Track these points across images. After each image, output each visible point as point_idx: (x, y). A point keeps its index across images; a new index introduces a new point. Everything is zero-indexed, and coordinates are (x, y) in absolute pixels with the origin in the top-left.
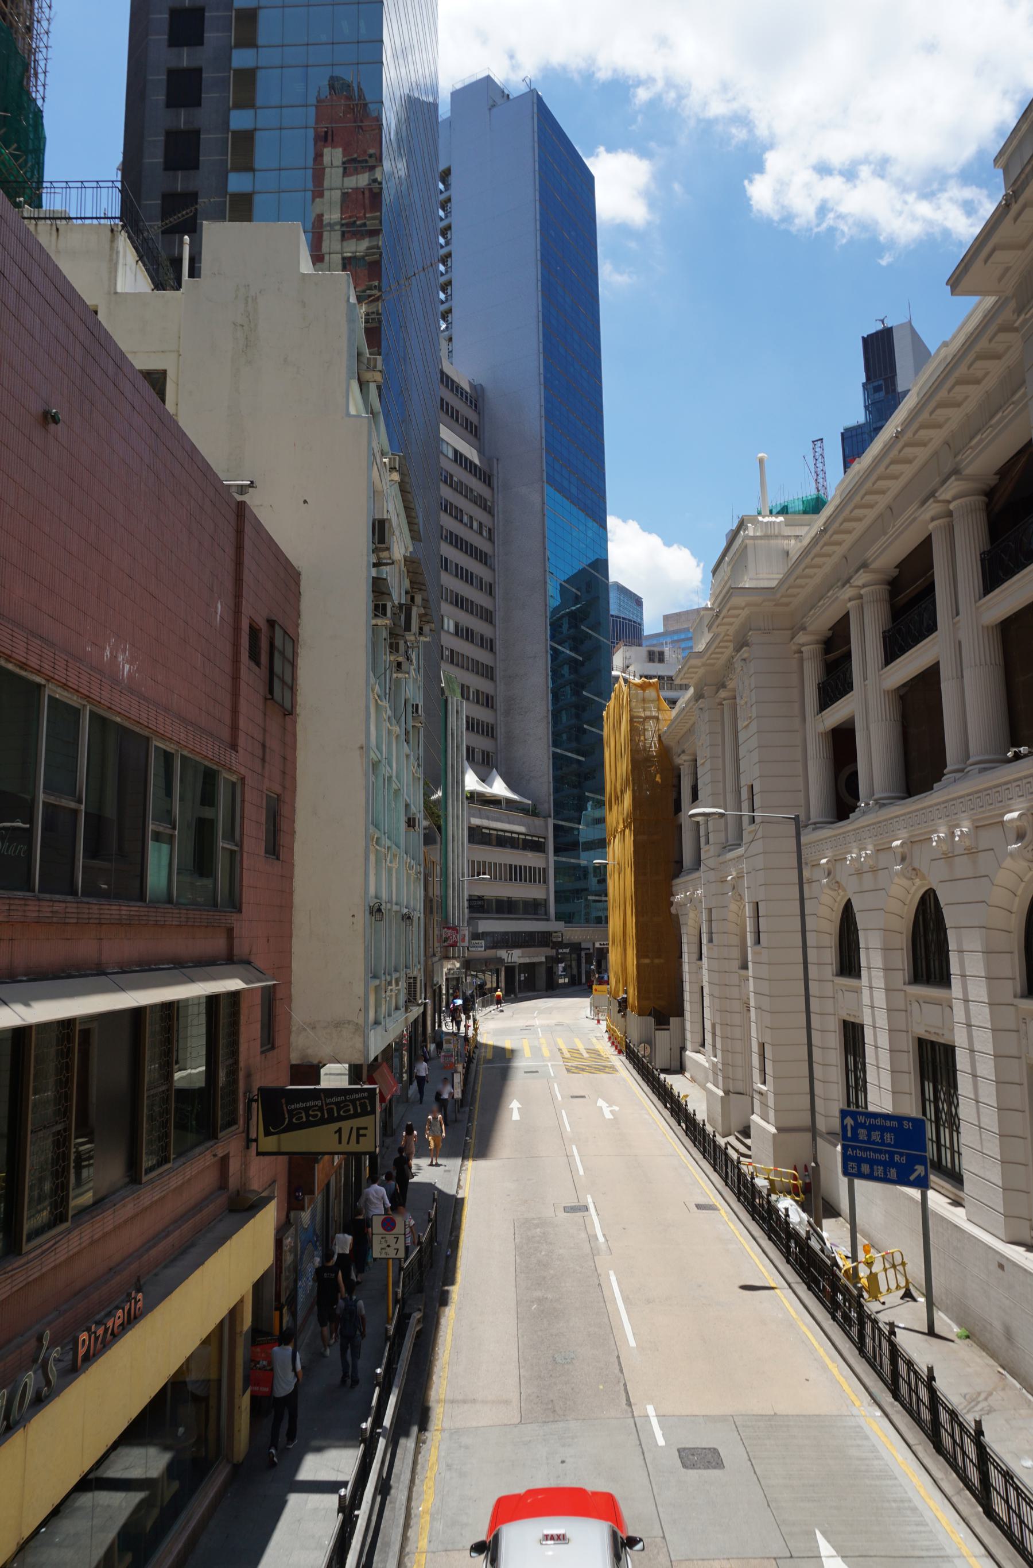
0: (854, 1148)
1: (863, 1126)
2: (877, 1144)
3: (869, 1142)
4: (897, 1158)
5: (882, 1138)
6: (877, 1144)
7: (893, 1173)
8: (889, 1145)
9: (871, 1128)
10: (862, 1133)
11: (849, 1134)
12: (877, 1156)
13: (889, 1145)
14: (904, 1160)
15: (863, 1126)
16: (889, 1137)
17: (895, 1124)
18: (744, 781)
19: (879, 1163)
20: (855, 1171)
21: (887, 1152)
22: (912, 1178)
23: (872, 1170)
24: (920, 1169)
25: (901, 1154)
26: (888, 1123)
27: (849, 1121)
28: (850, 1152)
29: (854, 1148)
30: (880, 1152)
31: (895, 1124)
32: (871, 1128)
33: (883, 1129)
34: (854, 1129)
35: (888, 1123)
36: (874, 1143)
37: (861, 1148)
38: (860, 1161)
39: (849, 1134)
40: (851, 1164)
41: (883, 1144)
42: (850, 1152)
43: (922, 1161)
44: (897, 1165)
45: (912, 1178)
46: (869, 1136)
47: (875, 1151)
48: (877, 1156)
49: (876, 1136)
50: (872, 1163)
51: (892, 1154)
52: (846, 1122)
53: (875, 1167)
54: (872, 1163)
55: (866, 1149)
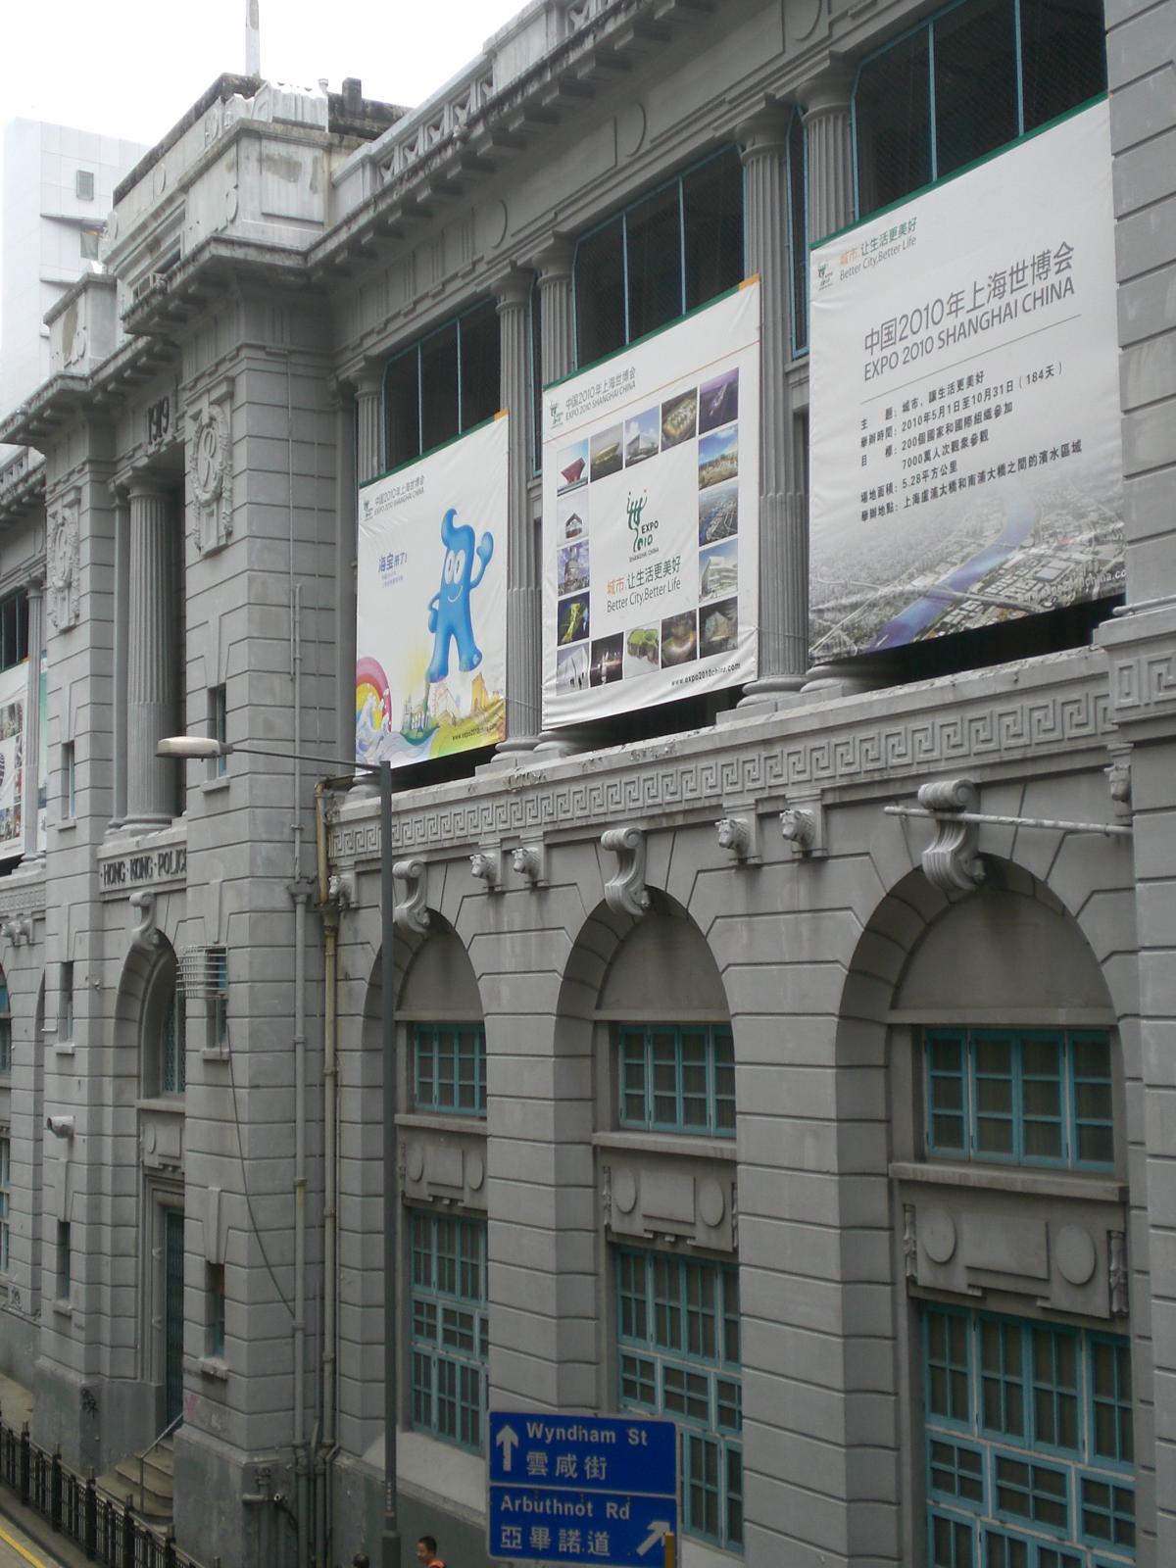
0: (516, 1494)
2: (570, 1481)
3: (551, 1478)
4: (611, 1509)
5: (580, 1468)
6: (570, 1481)
7: (601, 1543)
8: (595, 1483)
9: (556, 1449)
10: (537, 1461)
11: (507, 1465)
12: (569, 1508)
13: (595, 1483)
14: (625, 1513)
15: (538, 1444)
16: (595, 1466)
17: (610, 1436)
18: (198, 679)
19: (571, 1522)
20: (517, 1544)
21: (588, 1497)
22: (642, 1549)
23: (555, 1539)
24: (660, 1529)
25: (621, 1501)
26: (595, 1436)
27: (508, 1436)
28: (507, 1503)
29: (516, 1494)
30: (575, 1498)
31: (610, 1436)
32: (556, 1449)
33: (583, 1449)
34: (519, 1455)
35: (595, 1436)
36: (563, 1480)
37: (531, 1494)
38: (526, 1521)
39: (507, 1465)
40: (507, 1529)
41: (582, 1479)
42: (507, 1503)
43: (667, 1512)
44: (615, 1528)
45: (642, 1549)
46: (551, 1465)
47: (563, 1497)
48: (569, 1508)
49: (566, 1465)
50: (555, 1523)
51: (600, 1502)
52: (500, 1438)
53: (562, 1532)
54: (555, 1523)
55: (543, 1495)
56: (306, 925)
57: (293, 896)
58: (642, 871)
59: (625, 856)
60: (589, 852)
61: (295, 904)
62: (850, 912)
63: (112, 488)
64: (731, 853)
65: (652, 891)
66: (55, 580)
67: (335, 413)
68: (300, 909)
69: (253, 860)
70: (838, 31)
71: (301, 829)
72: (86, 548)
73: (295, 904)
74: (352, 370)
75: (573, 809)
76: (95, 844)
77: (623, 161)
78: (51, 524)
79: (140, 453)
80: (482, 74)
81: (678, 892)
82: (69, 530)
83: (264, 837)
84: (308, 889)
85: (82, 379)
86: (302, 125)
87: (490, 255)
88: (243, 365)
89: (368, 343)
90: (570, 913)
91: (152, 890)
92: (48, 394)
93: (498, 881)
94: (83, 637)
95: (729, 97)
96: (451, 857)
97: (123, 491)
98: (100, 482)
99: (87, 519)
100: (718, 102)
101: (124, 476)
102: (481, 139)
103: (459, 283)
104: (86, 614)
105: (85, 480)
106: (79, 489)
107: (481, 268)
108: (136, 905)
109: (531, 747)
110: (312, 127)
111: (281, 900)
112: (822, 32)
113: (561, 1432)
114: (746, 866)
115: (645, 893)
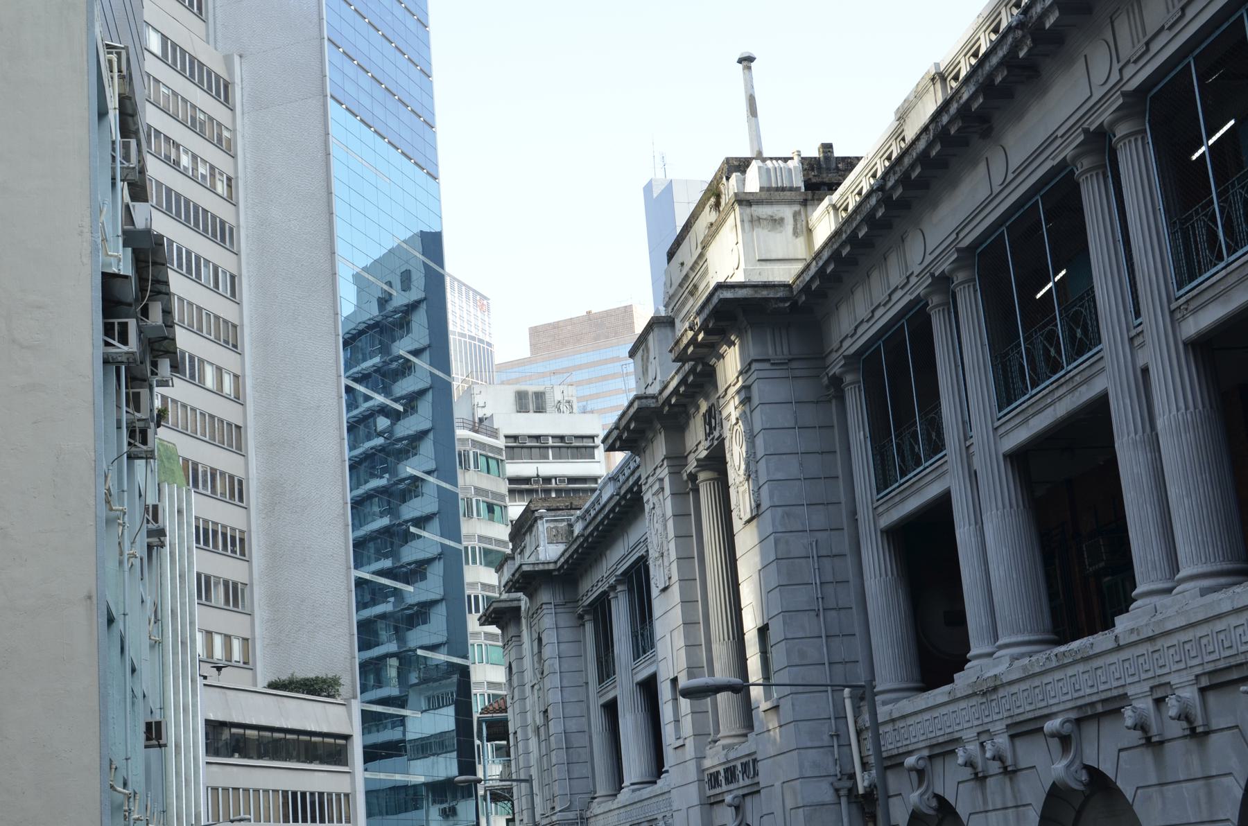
56: (849, 814)
57: (837, 790)
58: (1079, 752)
59: (1065, 741)
60: (1039, 740)
61: (839, 797)
62: (1230, 778)
63: (685, 477)
64: (1138, 733)
65: (1088, 768)
66: (653, 554)
67: (830, 401)
68: (844, 800)
69: (801, 766)
70: (1128, 73)
71: (838, 736)
72: (670, 524)
73: (839, 797)
74: (836, 370)
75: (1023, 704)
76: (700, 758)
77: (997, 189)
78: (647, 508)
79: (701, 447)
80: (898, 134)
81: (1107, 768)
82: (658, 511)
83: (809, 744)
84: (849, 784)
85: (653, 397)
86: (783, 189)
87: (917, 270)
88: (754, 376)
89: (846, 345)
90: (1033, 794)
91: (741, 792)
92: (632, 411)
93: (980, 769)
94: (675, 590)
95: (1060, 133)
96: (943, 751)
97: (693, 477)
98: (675, 473)
99: (669, 503)
100: (1052, 139)
101: (692, 466)
102: (894, 187)
103: (899, 293)
104: (675, 577)
105: (664, 472)
106: (661, 480)
107: (913, 280)
108: (730, 806)
109: (990, 655)
110: (791, 189)
111: (828, 796)
112: (1115, 77)
114: (1154, 744)
115: (1084, 771)
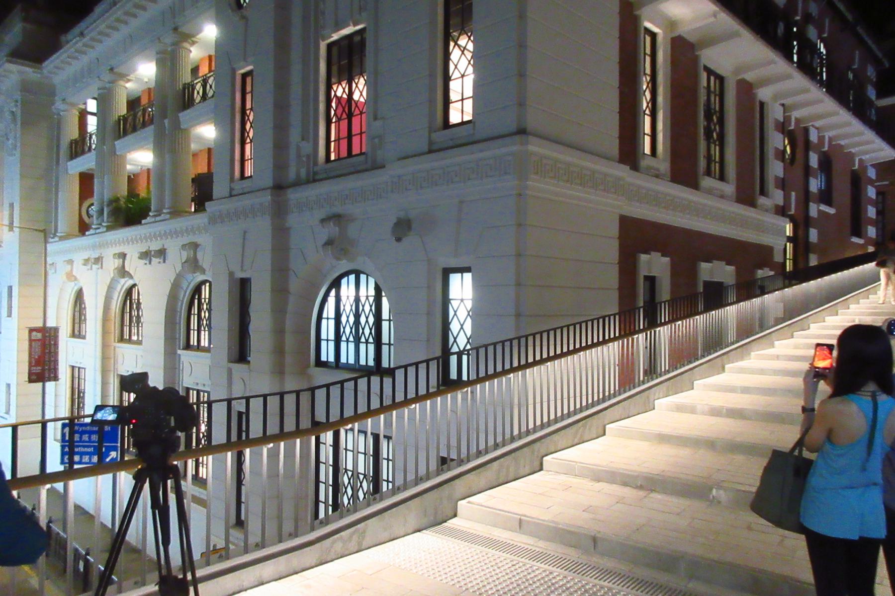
1: (77, 432)
9: (82, 433)
15: (77, 432)
41: (90, 441)
47: (84, 447)
113: (84, 428)
